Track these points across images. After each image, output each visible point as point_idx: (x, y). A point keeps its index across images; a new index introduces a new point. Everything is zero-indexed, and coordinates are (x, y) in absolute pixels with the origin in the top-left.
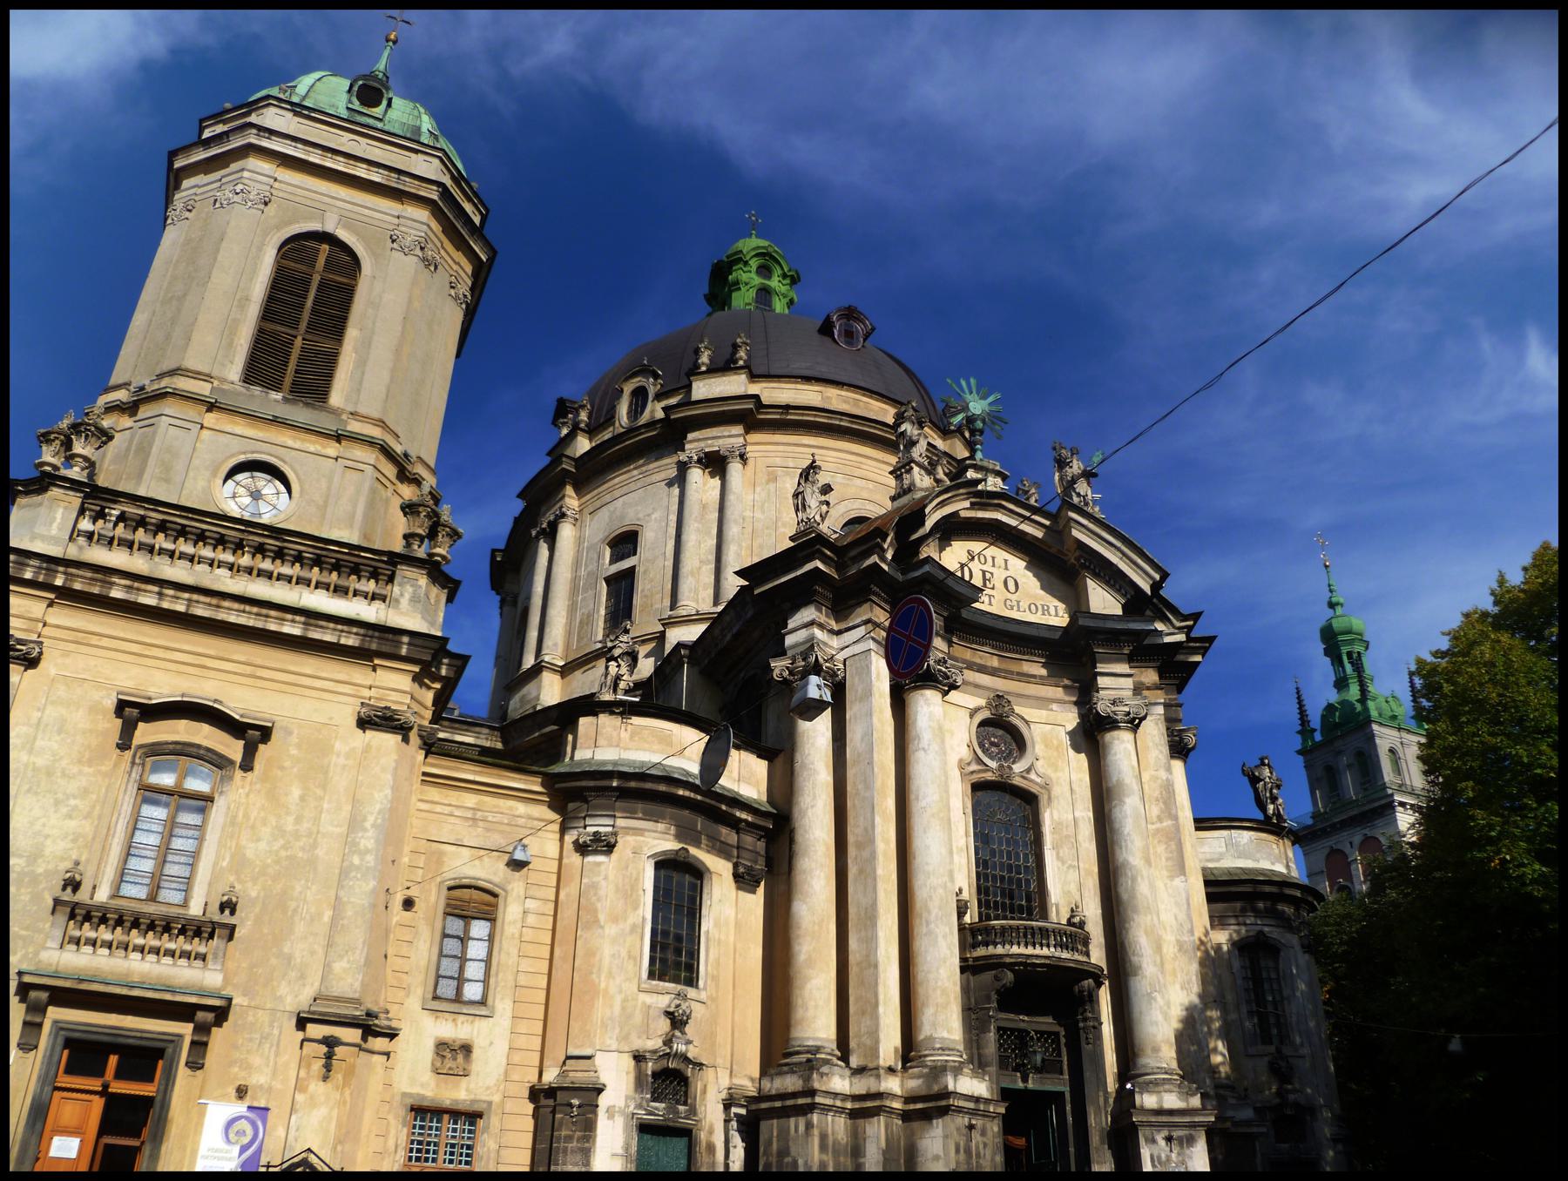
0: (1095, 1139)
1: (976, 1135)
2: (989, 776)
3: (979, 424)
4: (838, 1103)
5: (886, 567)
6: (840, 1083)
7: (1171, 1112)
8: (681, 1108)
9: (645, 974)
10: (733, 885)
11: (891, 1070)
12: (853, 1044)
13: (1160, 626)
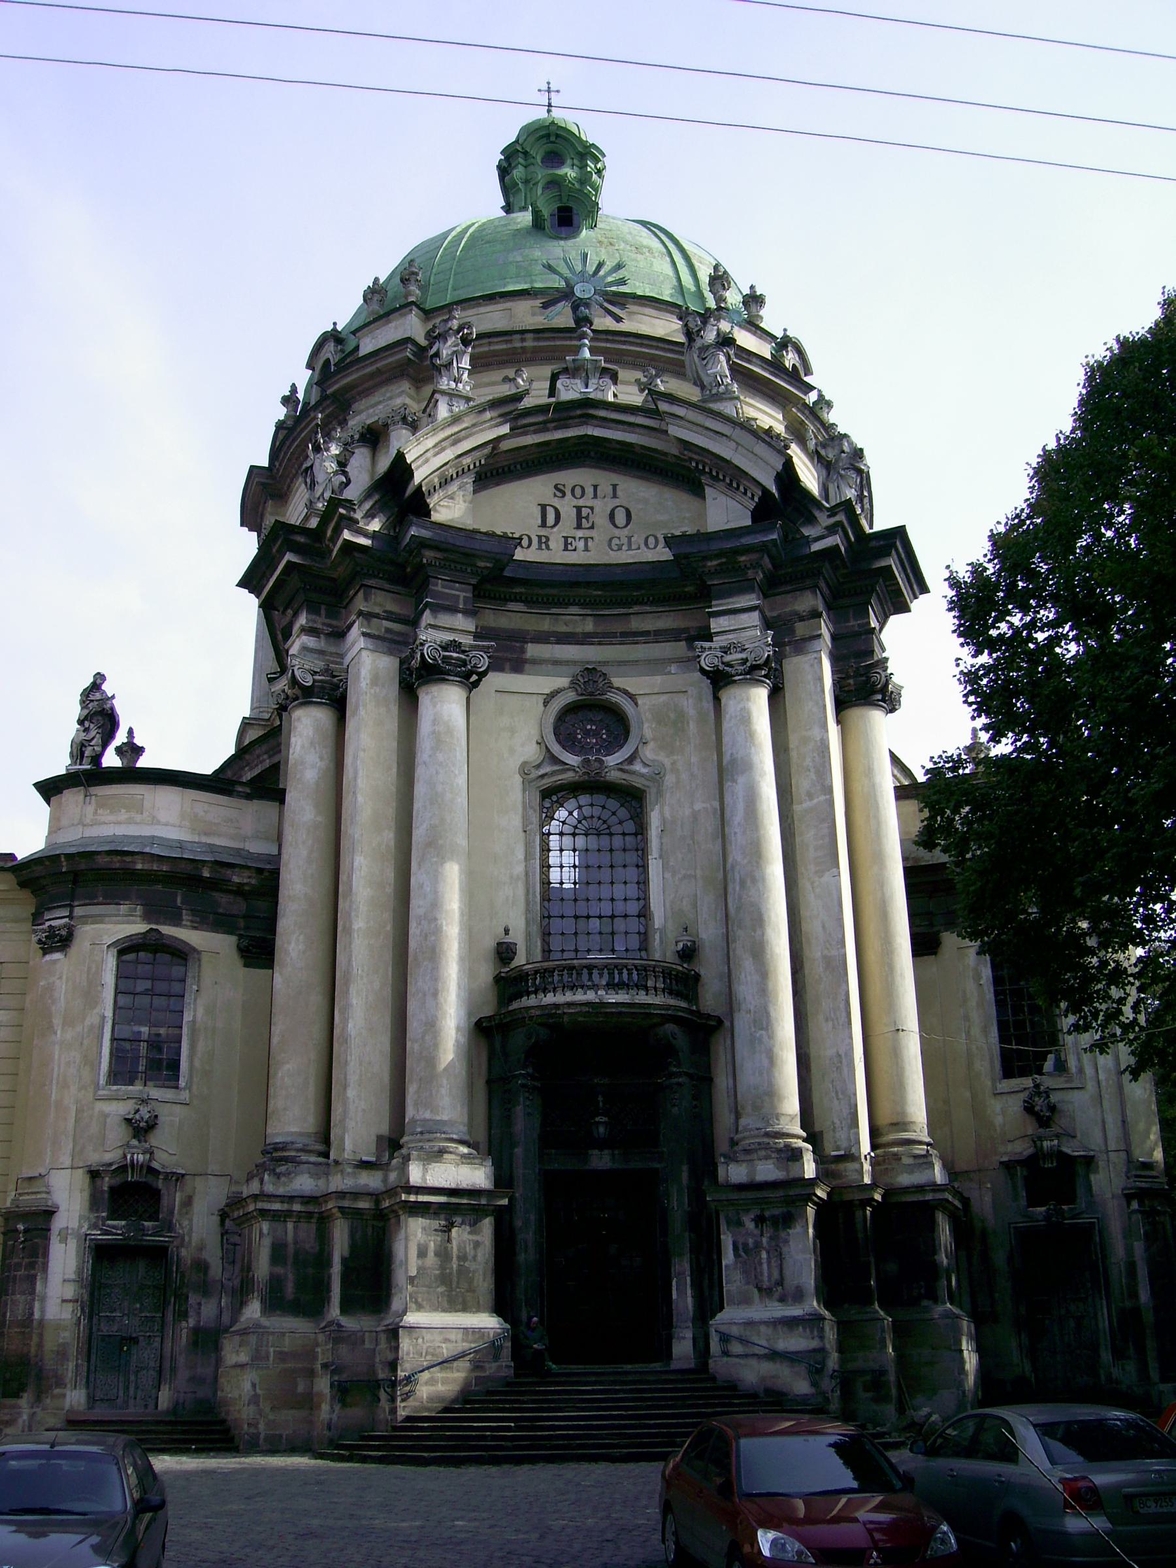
2: (569, 776)
4: (297, 1207)
5: (367, 542)
6: (304, 1183)
8: (146, 1223)
9: (102, 1081)
10: (238, 962)
11: (364, 1165)
13: (807, 531)
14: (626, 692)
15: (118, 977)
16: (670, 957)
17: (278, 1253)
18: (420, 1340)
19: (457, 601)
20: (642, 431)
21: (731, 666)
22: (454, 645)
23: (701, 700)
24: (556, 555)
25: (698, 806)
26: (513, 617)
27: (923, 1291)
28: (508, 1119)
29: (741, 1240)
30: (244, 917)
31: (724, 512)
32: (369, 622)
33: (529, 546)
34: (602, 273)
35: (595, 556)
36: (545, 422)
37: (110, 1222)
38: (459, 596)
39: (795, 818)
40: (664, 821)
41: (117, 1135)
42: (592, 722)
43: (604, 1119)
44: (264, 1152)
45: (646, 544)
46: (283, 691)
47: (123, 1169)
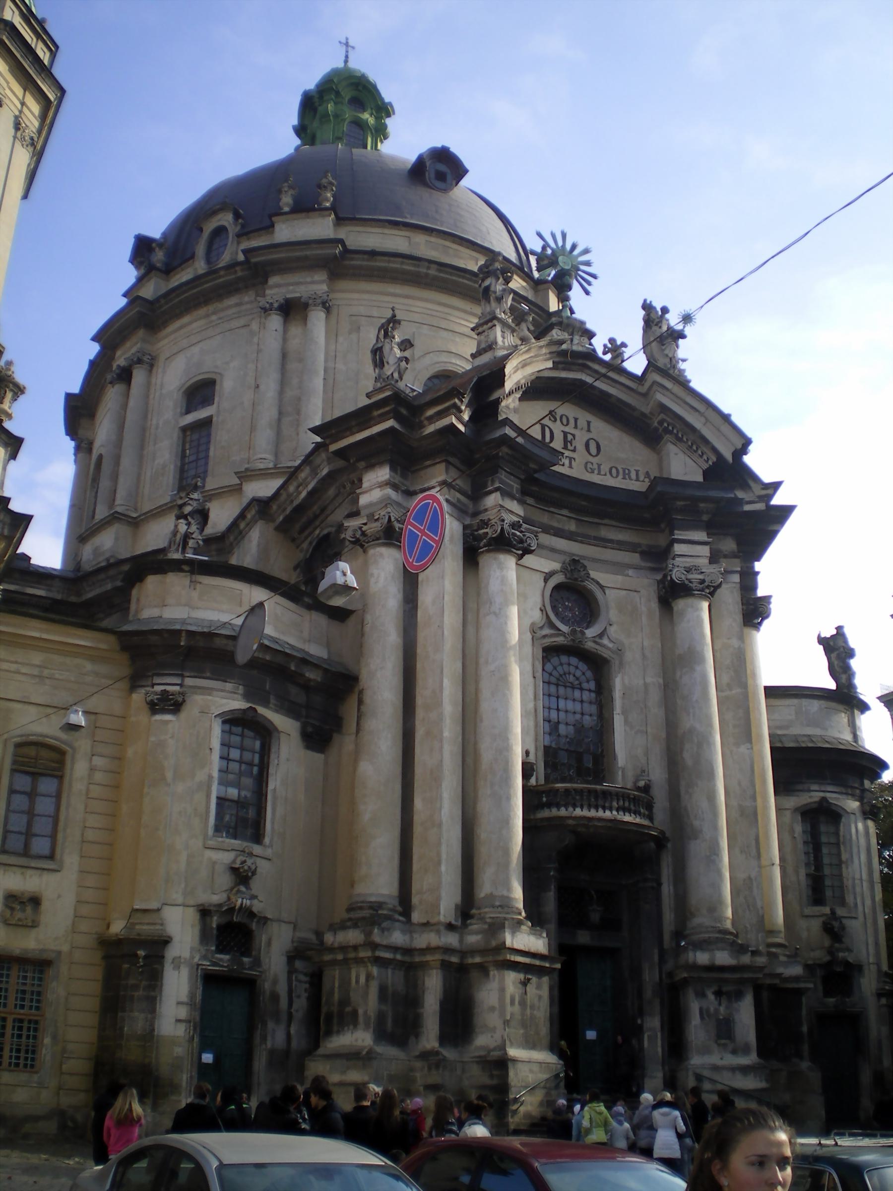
0: (648, 993)
1: (531, 989)
2: (560, 640)
4: (399, 957)
5: (462, 428)
6: (398, 937)
7: (722, 969)
8: (246, 960)
9: (211, 831)
11: (450, 927)
12: (415, 900)
13: (740, 494)
14: (598, 583)
15: (222, 744)
21: (691, 582)
25: (649, 680)
31: (683, 467)
34: (576, 252)
37: (218, 956)
38: (512, 487)
41: (225, 880)
46: (360, 528)
47: (231, 910)
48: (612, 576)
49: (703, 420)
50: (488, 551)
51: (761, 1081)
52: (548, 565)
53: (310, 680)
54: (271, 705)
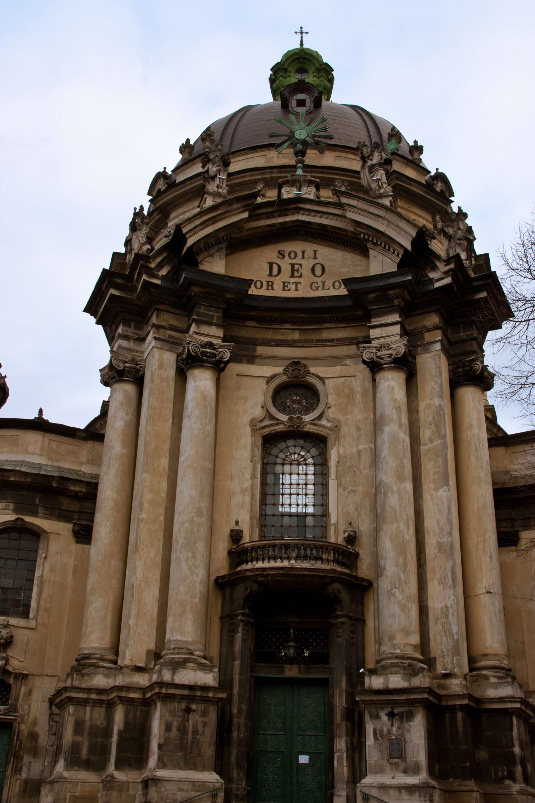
0: (338, 716)
1: (194, 719)
3: (299, 147)
4: (93, 696)
5: (158, 282)
6: (100, 681)
11: (139, 669)
13: (432, 275)
14: (318, 377)
16: (340, 540)
17: (78, 728)
18: (162, 789)
19: (213, 319)
20: (332, 217)
21: (381, 358)
22: (210, 345)
23: (365, 381)
24: (278, 292)
25: (361, 447)
26: (250, 331)
27: (505, 773)
28: (232, 642)
29: (378, 728)
30: (78, 512)
32: (158, 331)
33: (261, 287)
35: (300, 294)
36: (272, 213)
38: (213, 316)
39: (422, 454)
40: (339, 455)
42: (297, 395)
43: (293, 644)
44: (77, 660)
45: (334, 287)
48: (332, 368)
49: (386, 222)
50: (188, 369)
51: (425, 801)
52: (268, 371)
53: (77, 492)
54: (39, 515)
